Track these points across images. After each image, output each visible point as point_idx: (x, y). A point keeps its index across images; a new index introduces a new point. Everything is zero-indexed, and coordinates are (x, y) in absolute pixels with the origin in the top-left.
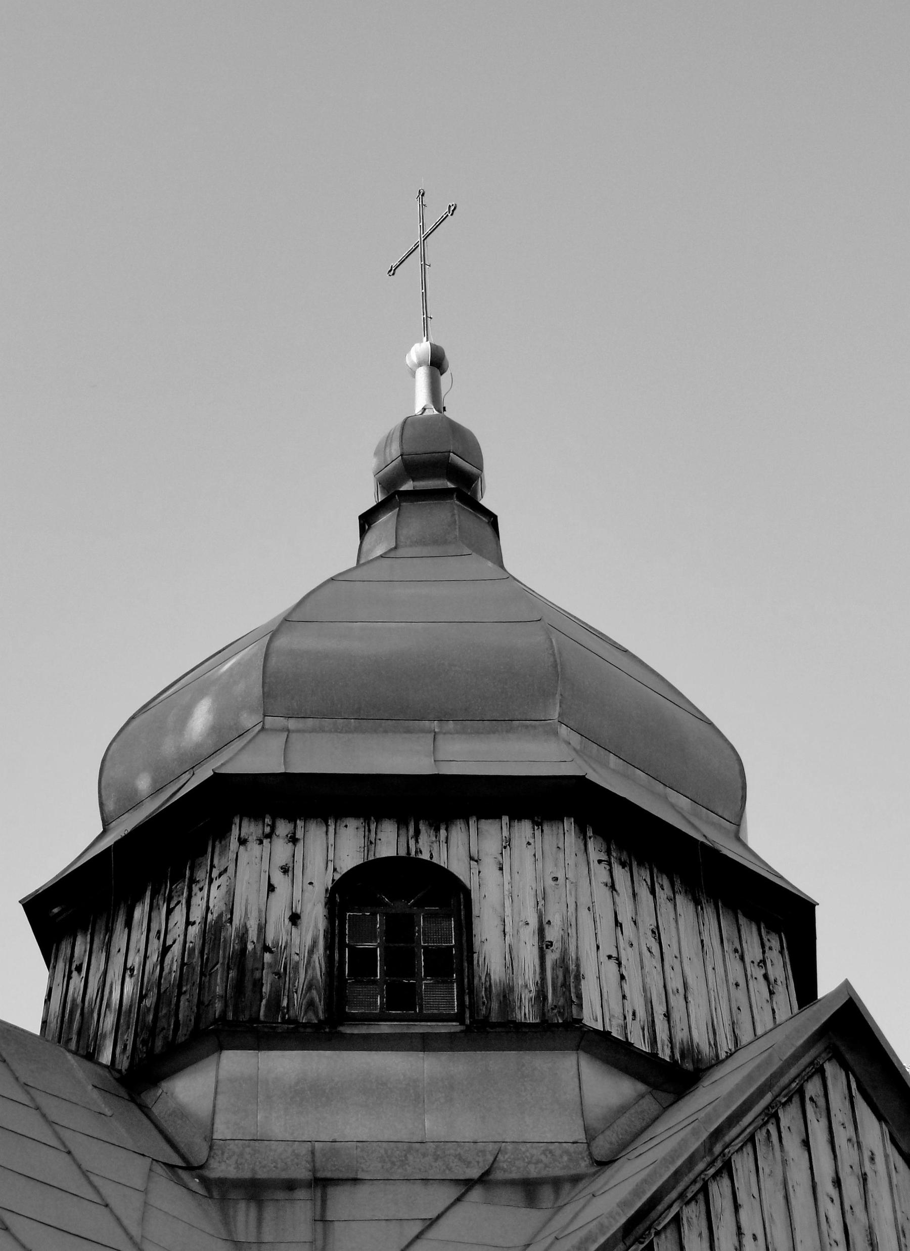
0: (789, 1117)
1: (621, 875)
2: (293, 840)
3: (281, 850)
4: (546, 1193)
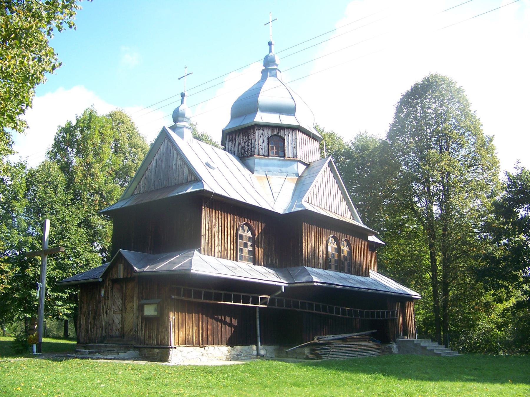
2: (263, 130)
3: (261, 131)
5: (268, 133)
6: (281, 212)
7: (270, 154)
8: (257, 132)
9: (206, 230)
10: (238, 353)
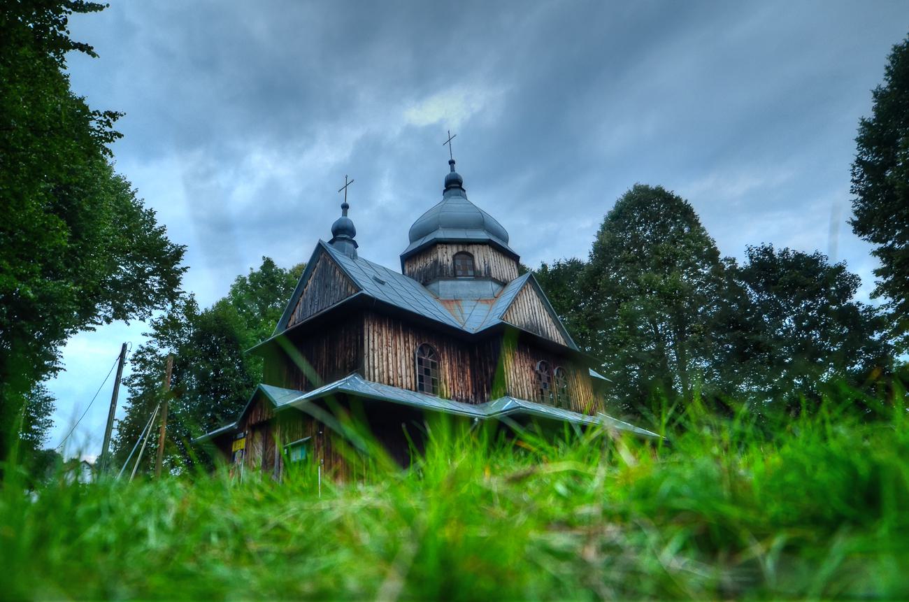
5: (453, 250)
6: (472, 332)
8: (440, 251)
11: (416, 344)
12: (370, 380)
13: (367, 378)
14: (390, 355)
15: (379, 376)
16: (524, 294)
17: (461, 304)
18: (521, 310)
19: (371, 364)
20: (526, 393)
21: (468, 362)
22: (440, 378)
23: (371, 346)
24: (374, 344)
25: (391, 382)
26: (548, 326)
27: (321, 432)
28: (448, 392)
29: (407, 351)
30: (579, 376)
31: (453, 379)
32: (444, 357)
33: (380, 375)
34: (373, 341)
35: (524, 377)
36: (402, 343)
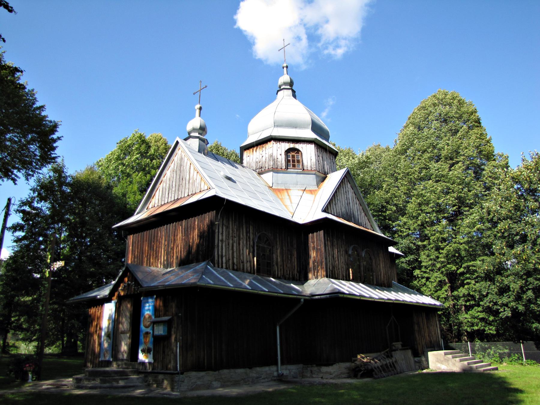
0: (341, 185)
1: (319, 150)
4: (313, 192)
7: (288, 168)
9: (219, 241)
10: (257, 375)
11: (255, 234)
12: (218, 267)
13: (216, 265)
14: (235, 244)
15: (226, 263)
16: (342, 187)
17: (289, 191)
18: (339, 202)
19: (220, 253)
20: (341, 273)
21: (295, 246)
22: (273, 262)
23: (220, 238)
24: (222, 236)
25: (235, 267)
26: (359, 214)
27: (180, 314)
28: (279, 273)
29: (248, 240)
30: (381, 255)
31: (283, 261)
32: (276, 243)
33: (227, 261)
34: (222, 234)
35: (340, 260)
36: (245, 234)
